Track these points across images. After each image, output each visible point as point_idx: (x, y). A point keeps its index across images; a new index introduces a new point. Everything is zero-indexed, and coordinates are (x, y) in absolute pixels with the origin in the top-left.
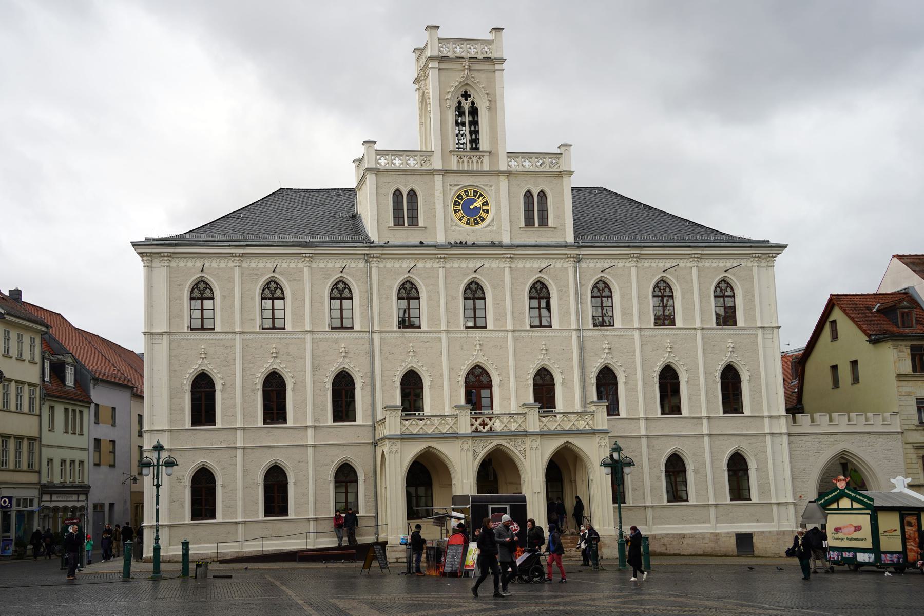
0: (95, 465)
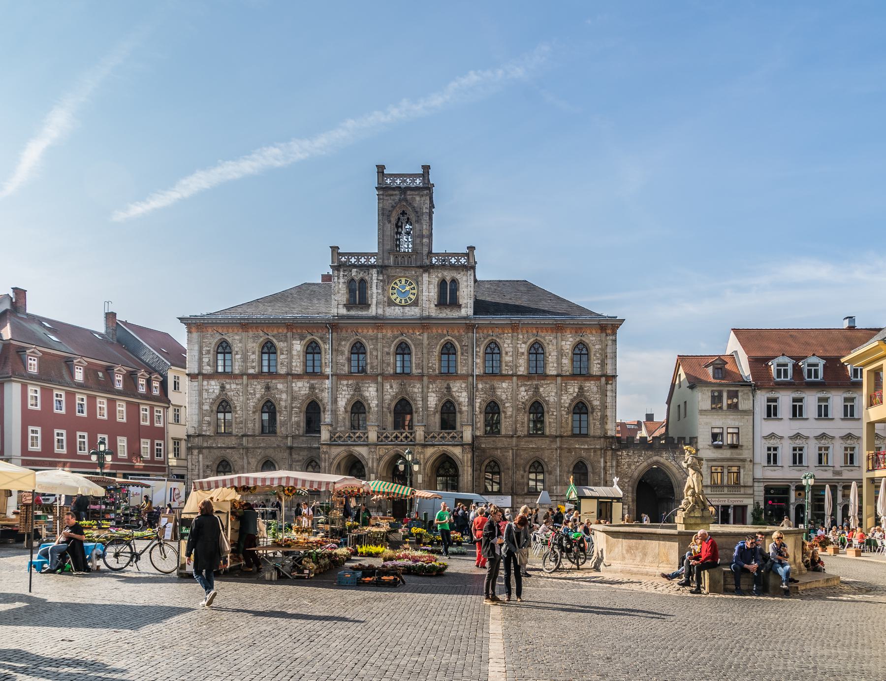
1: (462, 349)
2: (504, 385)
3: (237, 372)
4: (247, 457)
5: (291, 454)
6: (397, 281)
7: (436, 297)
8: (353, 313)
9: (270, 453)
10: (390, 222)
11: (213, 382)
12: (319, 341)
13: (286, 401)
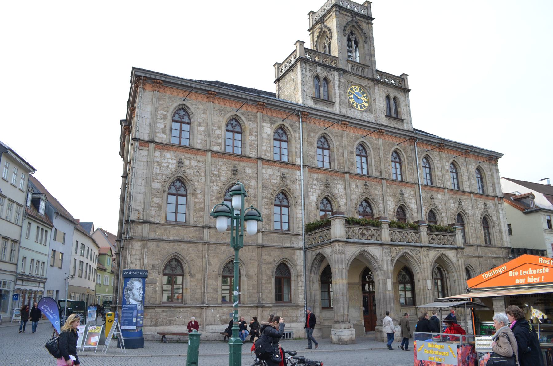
0: (51, 266)
1: (408, 159)
2: (440, 196)
3: (199, 146)
4: (208, 255)
5: (261, 255)
6: (353, 88)
7: (385, 109)
8: (320, 107)
10: (345, 35)
11: (168, 155)
12: (289, 128)
13: (255, 189)
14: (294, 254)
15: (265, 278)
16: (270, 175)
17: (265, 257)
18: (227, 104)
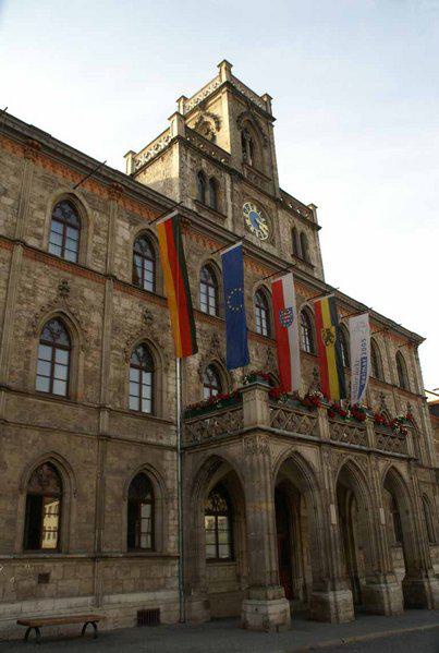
5: (104, 453)
9: (59, 443)
13: (102, 328)
14: (163, 458)
15: (110, 501)
16: (126, 310)
17: (111, 459)
18: (59, 172)
